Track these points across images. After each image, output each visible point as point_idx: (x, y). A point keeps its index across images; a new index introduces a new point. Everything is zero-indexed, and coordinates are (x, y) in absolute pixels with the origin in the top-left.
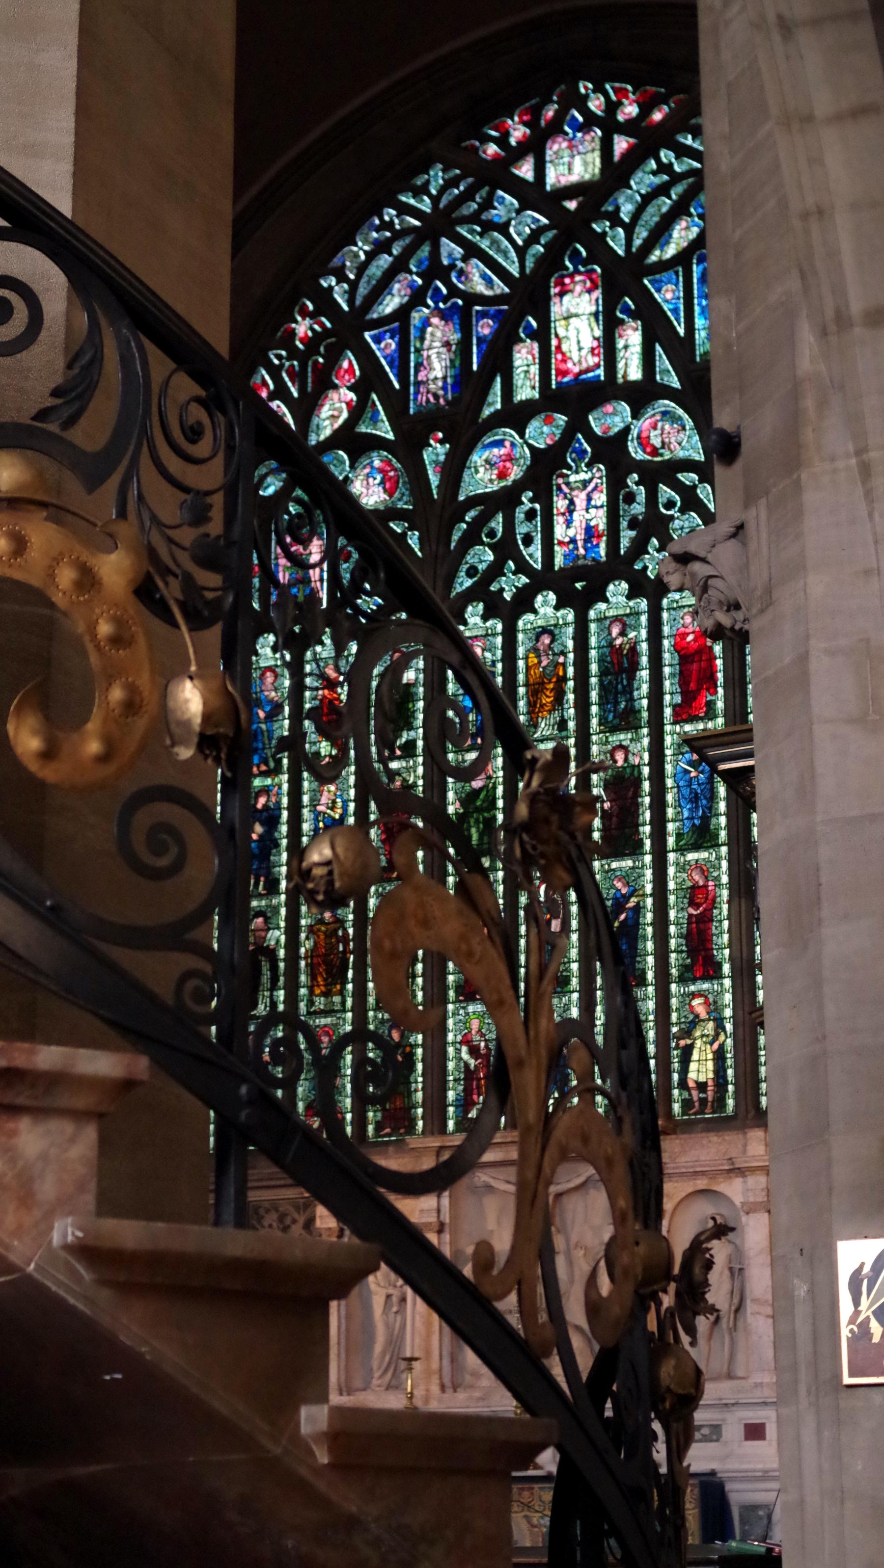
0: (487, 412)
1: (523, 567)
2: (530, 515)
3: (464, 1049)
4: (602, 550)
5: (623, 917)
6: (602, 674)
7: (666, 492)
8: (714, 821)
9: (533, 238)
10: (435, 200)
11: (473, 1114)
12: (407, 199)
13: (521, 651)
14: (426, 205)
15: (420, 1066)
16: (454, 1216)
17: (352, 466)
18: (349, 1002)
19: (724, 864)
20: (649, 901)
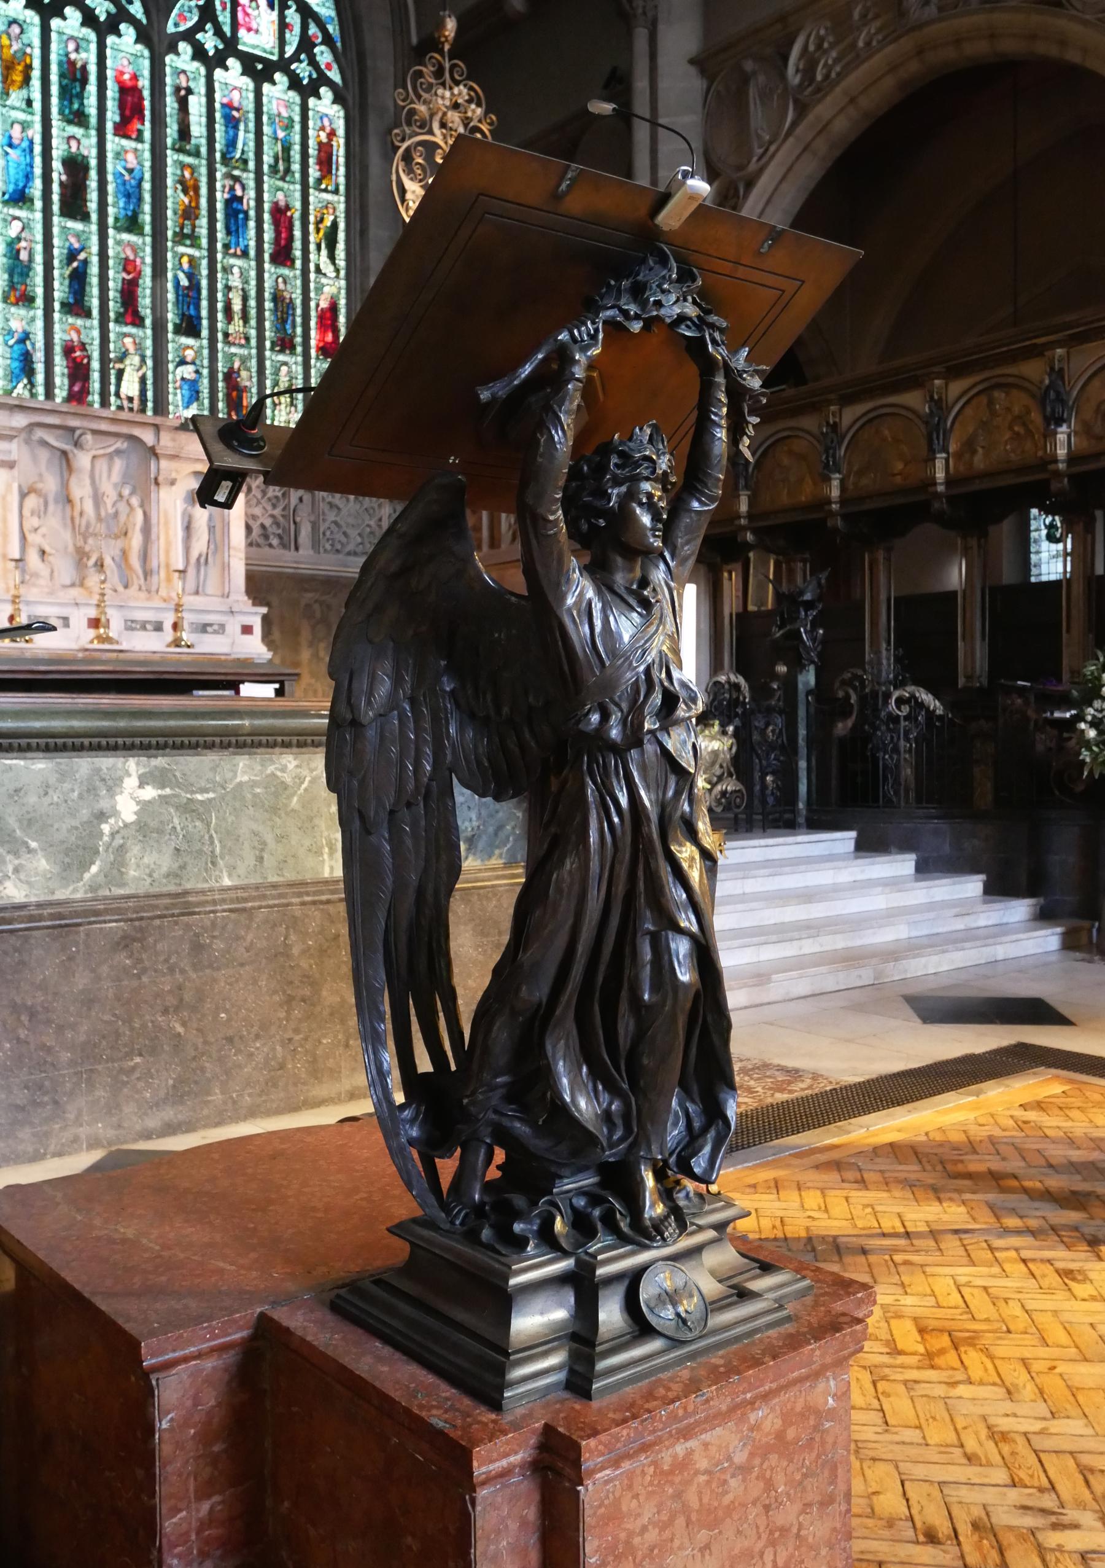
5: (75, 264)
6: (62, 76)
8: (141, 217)
19: (148, 250)
20: (95, 260)
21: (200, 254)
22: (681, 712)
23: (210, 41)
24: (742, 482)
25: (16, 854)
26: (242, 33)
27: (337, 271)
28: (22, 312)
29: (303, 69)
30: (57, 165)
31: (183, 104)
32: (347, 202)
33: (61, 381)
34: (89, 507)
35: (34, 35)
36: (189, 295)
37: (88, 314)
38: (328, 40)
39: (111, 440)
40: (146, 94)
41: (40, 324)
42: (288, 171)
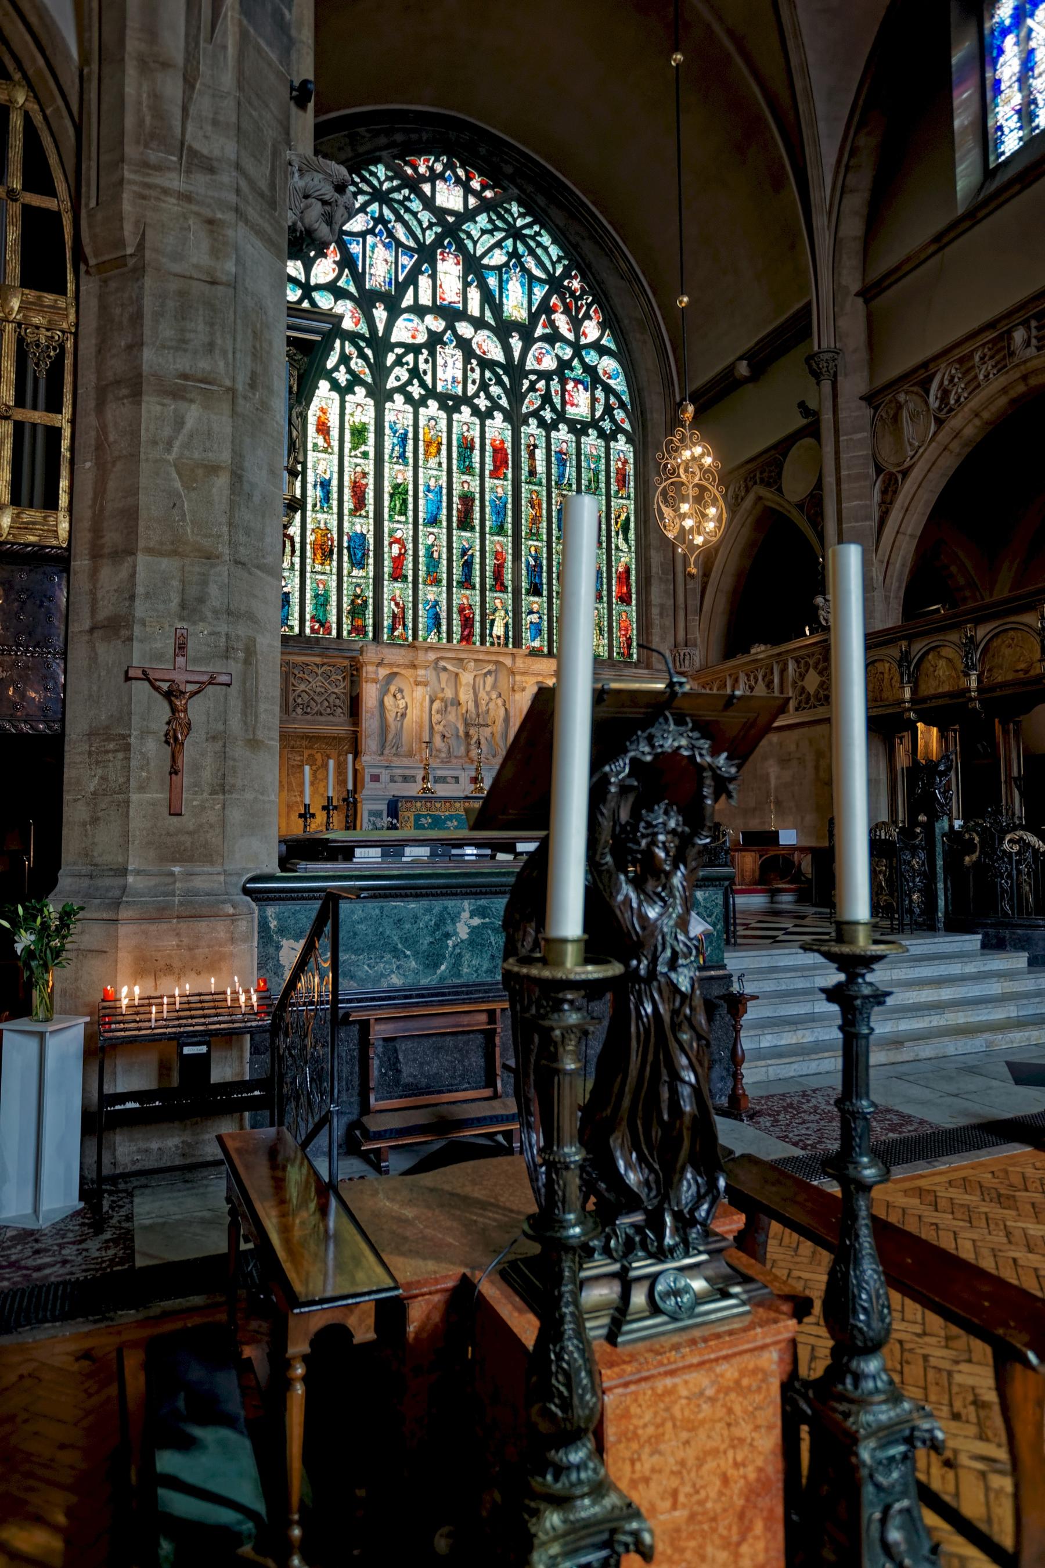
0: (404, 305)
2: (426, 361)
4: (459, 390)
7: (488, 374)
9: (431, 225)
18: (335, 570)
20: (478, 554)
21: (542, 545)
22: (681, 961)
23: (548, 415)
24: (905, 679)
25: (398, 959)
26: (568, 407)
27: (630, 547)
28: (435, 589)
29: (606, 425)
30: (455, 499)
31: (532, 455)
32: (636, 504)
33: (457, 628)
35: (443, 424)
36: (535, 570)
37: (474, 588)
38: (622, 405)
39: (485, 665)
40: (509, 451)
41: (444, 595)
42: (597, 488)
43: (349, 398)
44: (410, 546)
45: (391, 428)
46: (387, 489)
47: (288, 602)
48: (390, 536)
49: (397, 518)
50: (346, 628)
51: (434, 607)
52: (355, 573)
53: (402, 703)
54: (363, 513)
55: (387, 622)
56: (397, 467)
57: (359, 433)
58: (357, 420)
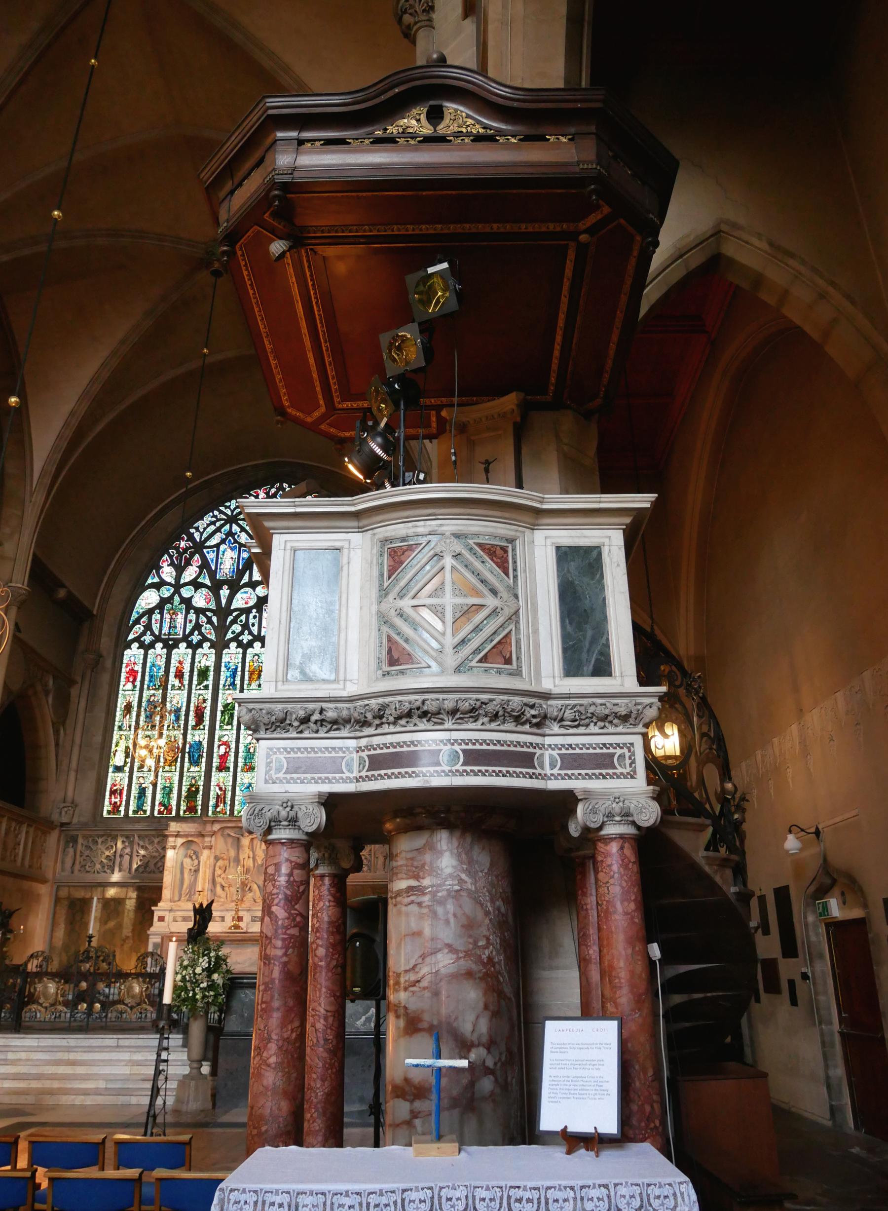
0: (243, 582)
1: (251, 633)
2: (255, 617)
3: (217, 788)
10: (232, 511)
11: (218, 810)
12: (222, 508)
13: (248, 660)
14: (229, 513)
15: (201, 793)
16: (216, 844)
17: (195, 592)
18: (178, 769)
28: (249, 774)
34: (250, 863)
43: (199, 651)
44: (233, 746)
45: (226, 667)
46: (220, 708)
47: (145, 794)
48: (219, 740)
49: (225, 727)
50: (183, 807)
51: (248, 788)
52: (193, 769)
53: (196, 862)
54: (202, 727)
55: (212, 802)
56: (228, 692)
57: (203, 674)
58: (203, 665)
